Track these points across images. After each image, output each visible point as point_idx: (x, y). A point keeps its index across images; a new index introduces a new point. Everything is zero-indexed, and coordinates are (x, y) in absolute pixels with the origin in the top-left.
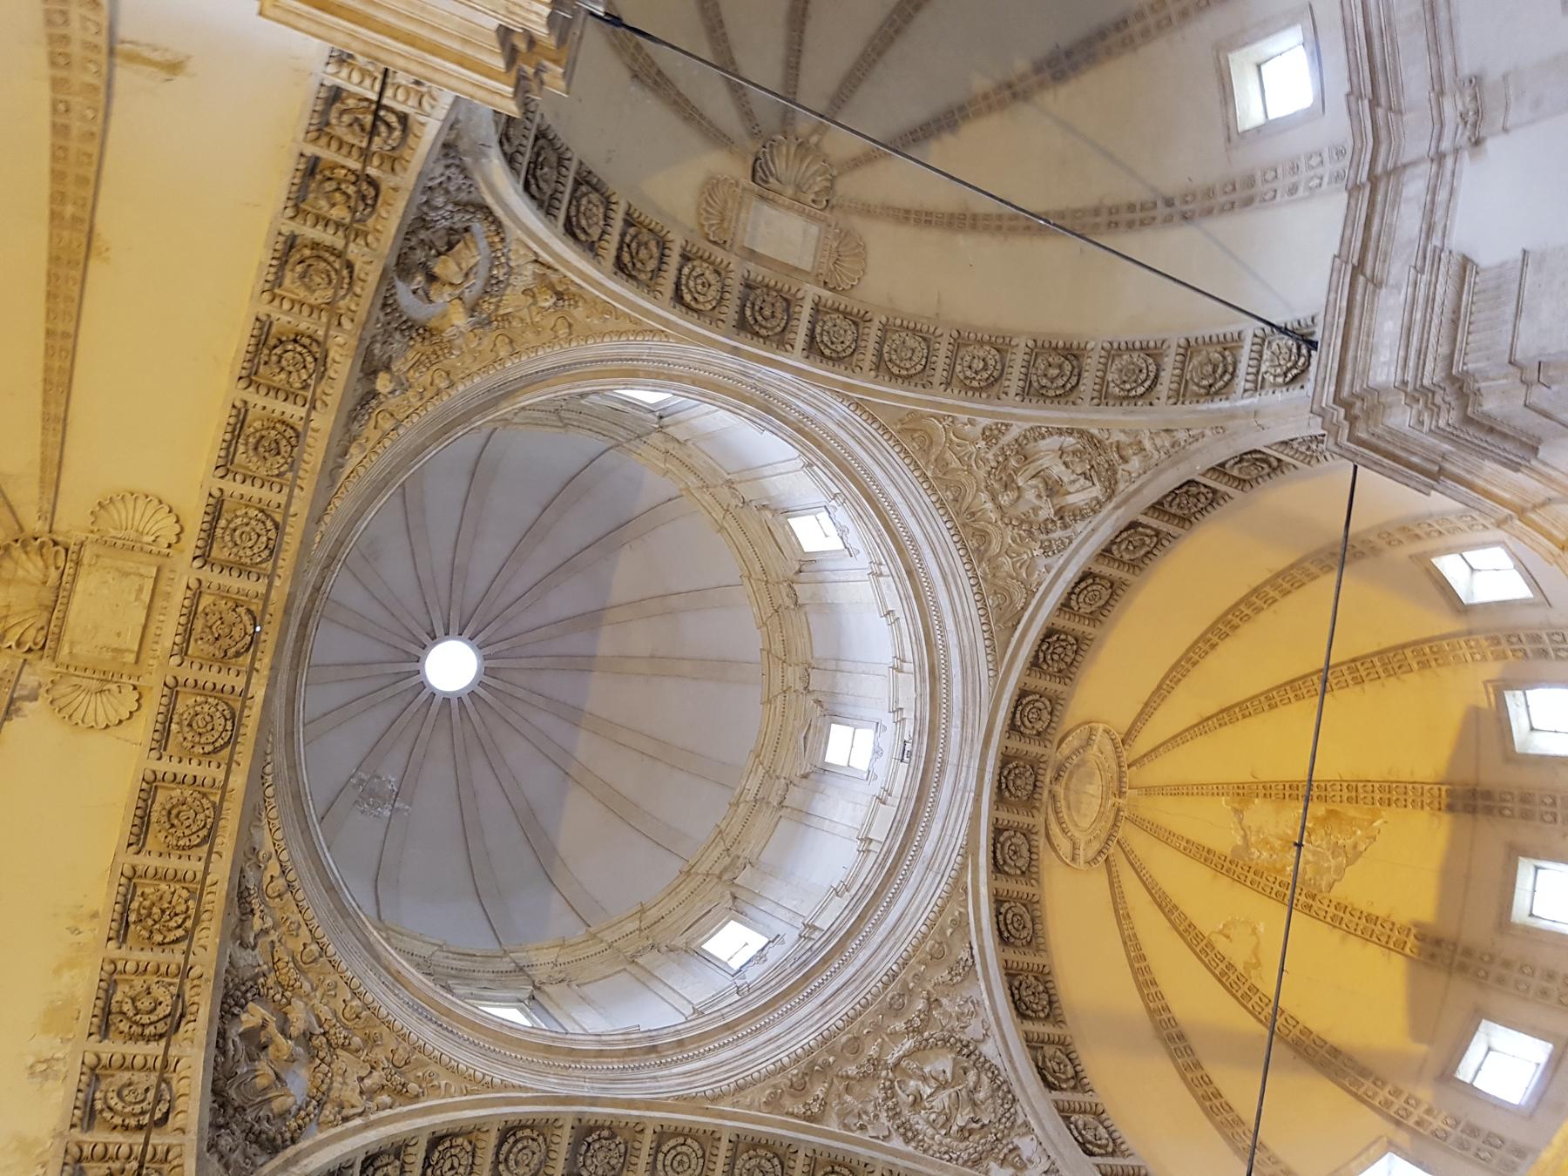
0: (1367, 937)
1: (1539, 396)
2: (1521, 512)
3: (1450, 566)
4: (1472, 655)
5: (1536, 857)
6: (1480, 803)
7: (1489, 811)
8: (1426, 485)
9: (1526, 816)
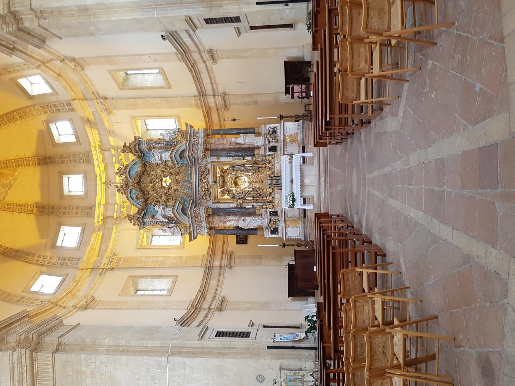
0: (20, 211)
1: (42, 22)
2: (44, 63)
3: (23, 82)
4: (37, 113)
5: (68, 174)
6: (48, 161)
7: (51, 163)
8: (9, 53)
9: (62, 162)
